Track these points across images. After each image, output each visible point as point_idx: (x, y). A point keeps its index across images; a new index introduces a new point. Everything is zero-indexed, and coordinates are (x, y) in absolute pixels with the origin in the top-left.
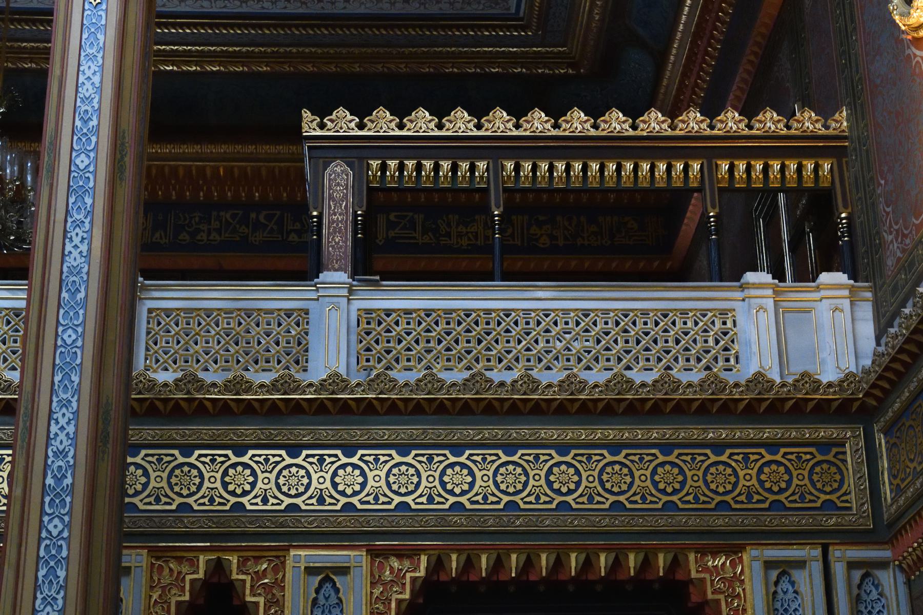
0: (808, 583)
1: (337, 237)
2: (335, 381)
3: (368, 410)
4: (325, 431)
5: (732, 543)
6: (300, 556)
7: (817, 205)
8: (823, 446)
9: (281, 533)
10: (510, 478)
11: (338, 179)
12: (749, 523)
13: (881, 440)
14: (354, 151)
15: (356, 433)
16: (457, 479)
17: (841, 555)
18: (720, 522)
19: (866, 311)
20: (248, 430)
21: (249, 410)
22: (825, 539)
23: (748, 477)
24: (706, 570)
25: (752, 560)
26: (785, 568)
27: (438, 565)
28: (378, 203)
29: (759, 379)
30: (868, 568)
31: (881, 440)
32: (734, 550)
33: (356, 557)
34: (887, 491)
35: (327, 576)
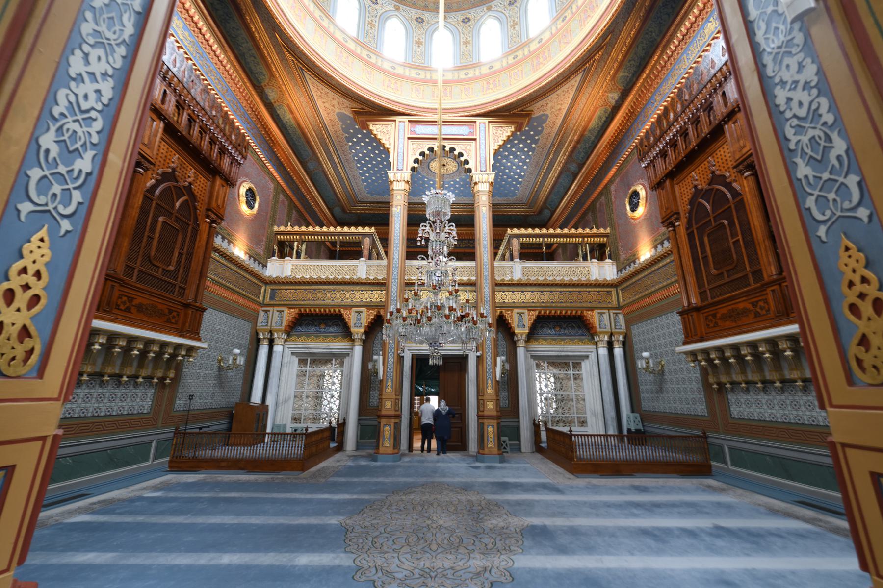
0: (606, 316)
1: (516, 254)
2: (521, 280)
3: (526, 285)
4: (519, 289)
5: (592, 309)
6: (516, 311)
7: (602, 246)
8: (608, 292)
9: (512, 307)
10: (552, 297)
11: (515, 242)
12: (595, 305)
13: (620, 291)
14: (518, 236)
15: (524, 289)
16: (543, 297)
17: (612, 311)
18: (590, 305)
19: (615, 267)
20: (505, 288)
21: (505, 285)
22: (609, 308)
23: (594, 297)
24: (588, 314)
25: (596, 312)
26: (601, 314)
27: (540, 312)
28: (523, 246)
29: (596, 280)
30: (616, 314)
31: (620, 291)
32: (592, 310)
33: (526, 311)
34: (621, 300)
35: (520, 314)
